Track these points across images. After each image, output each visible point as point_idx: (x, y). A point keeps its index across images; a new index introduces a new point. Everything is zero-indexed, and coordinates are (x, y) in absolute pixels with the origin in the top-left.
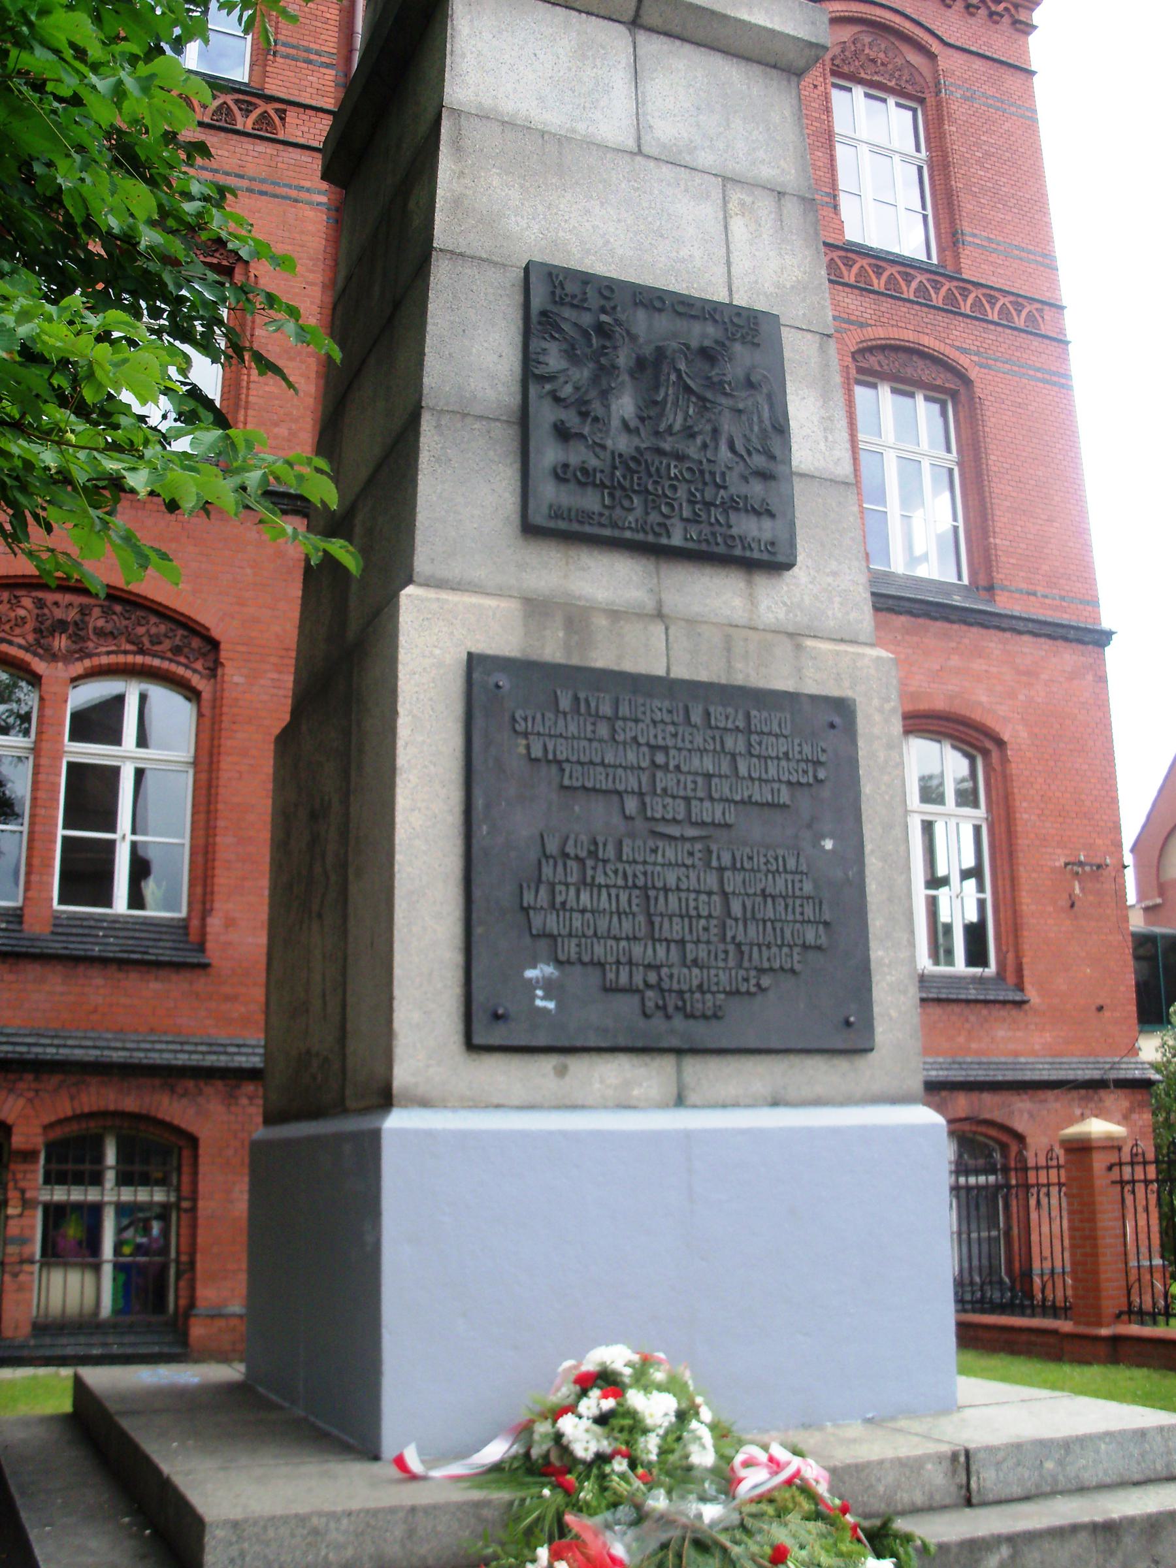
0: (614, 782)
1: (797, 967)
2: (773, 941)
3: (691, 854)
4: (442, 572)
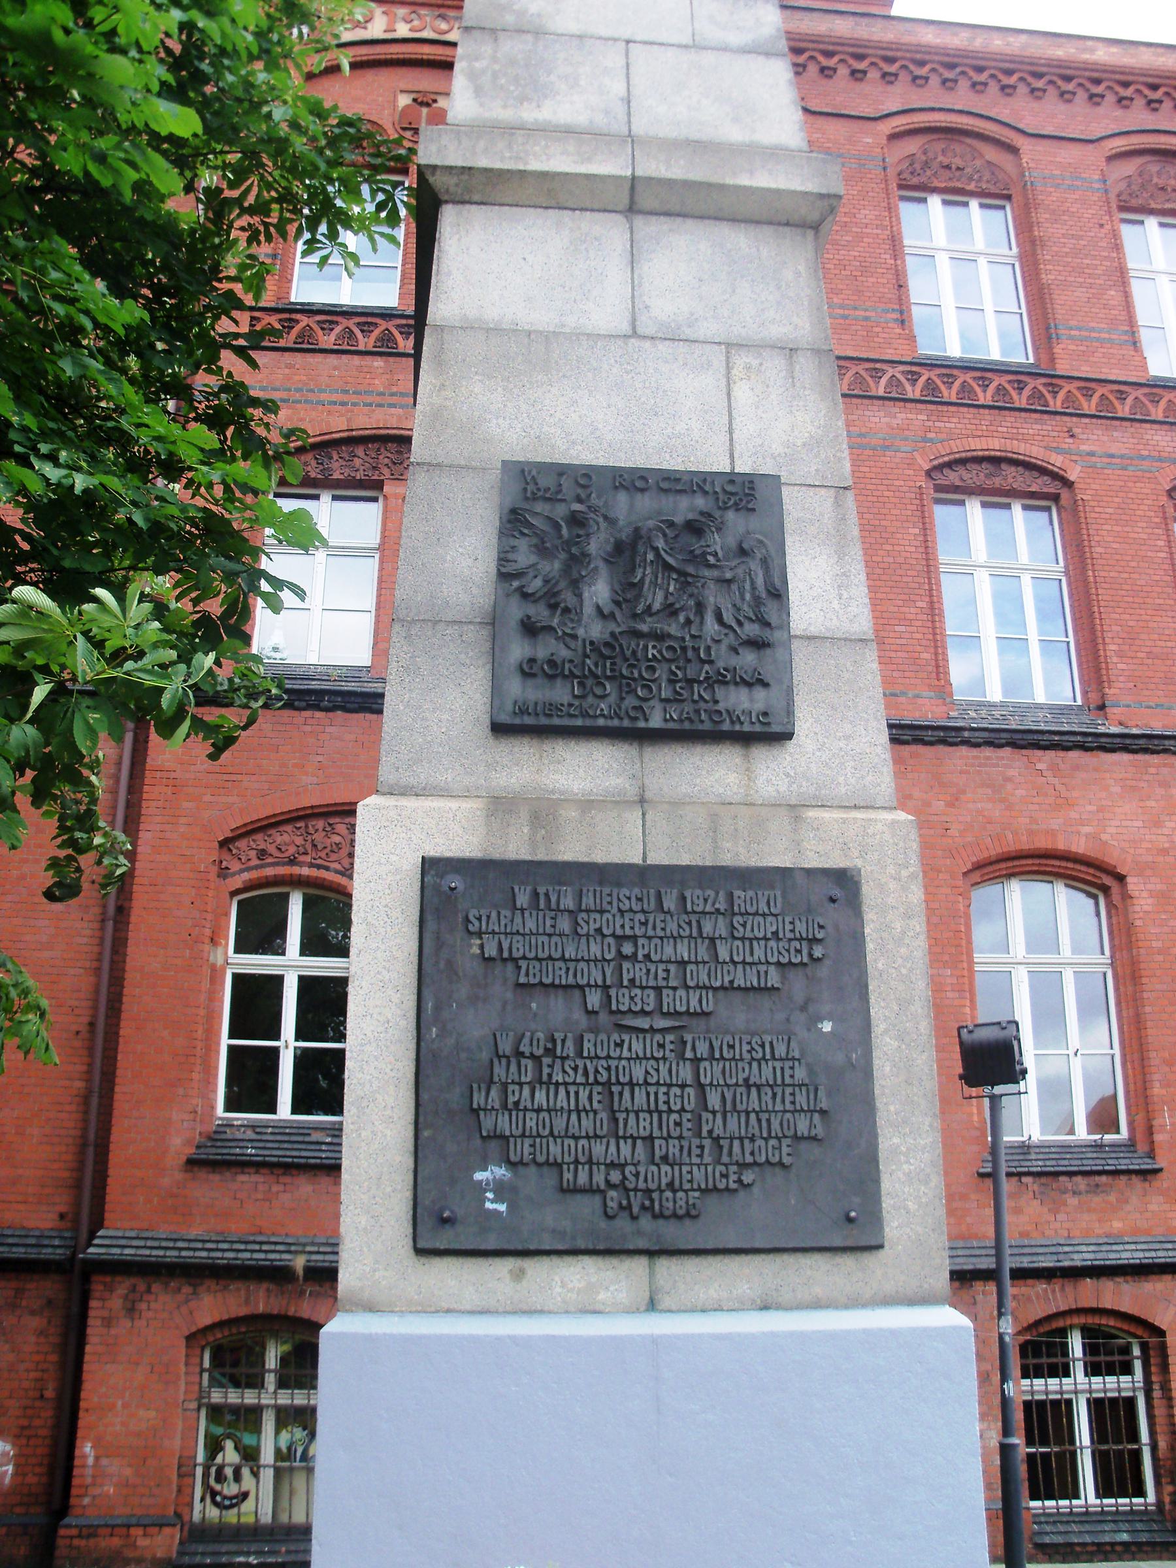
0: (575, 976)
1: (786, 1160)
2: (757, 1133)
3: (661, 1046)
4: (407, 778)
